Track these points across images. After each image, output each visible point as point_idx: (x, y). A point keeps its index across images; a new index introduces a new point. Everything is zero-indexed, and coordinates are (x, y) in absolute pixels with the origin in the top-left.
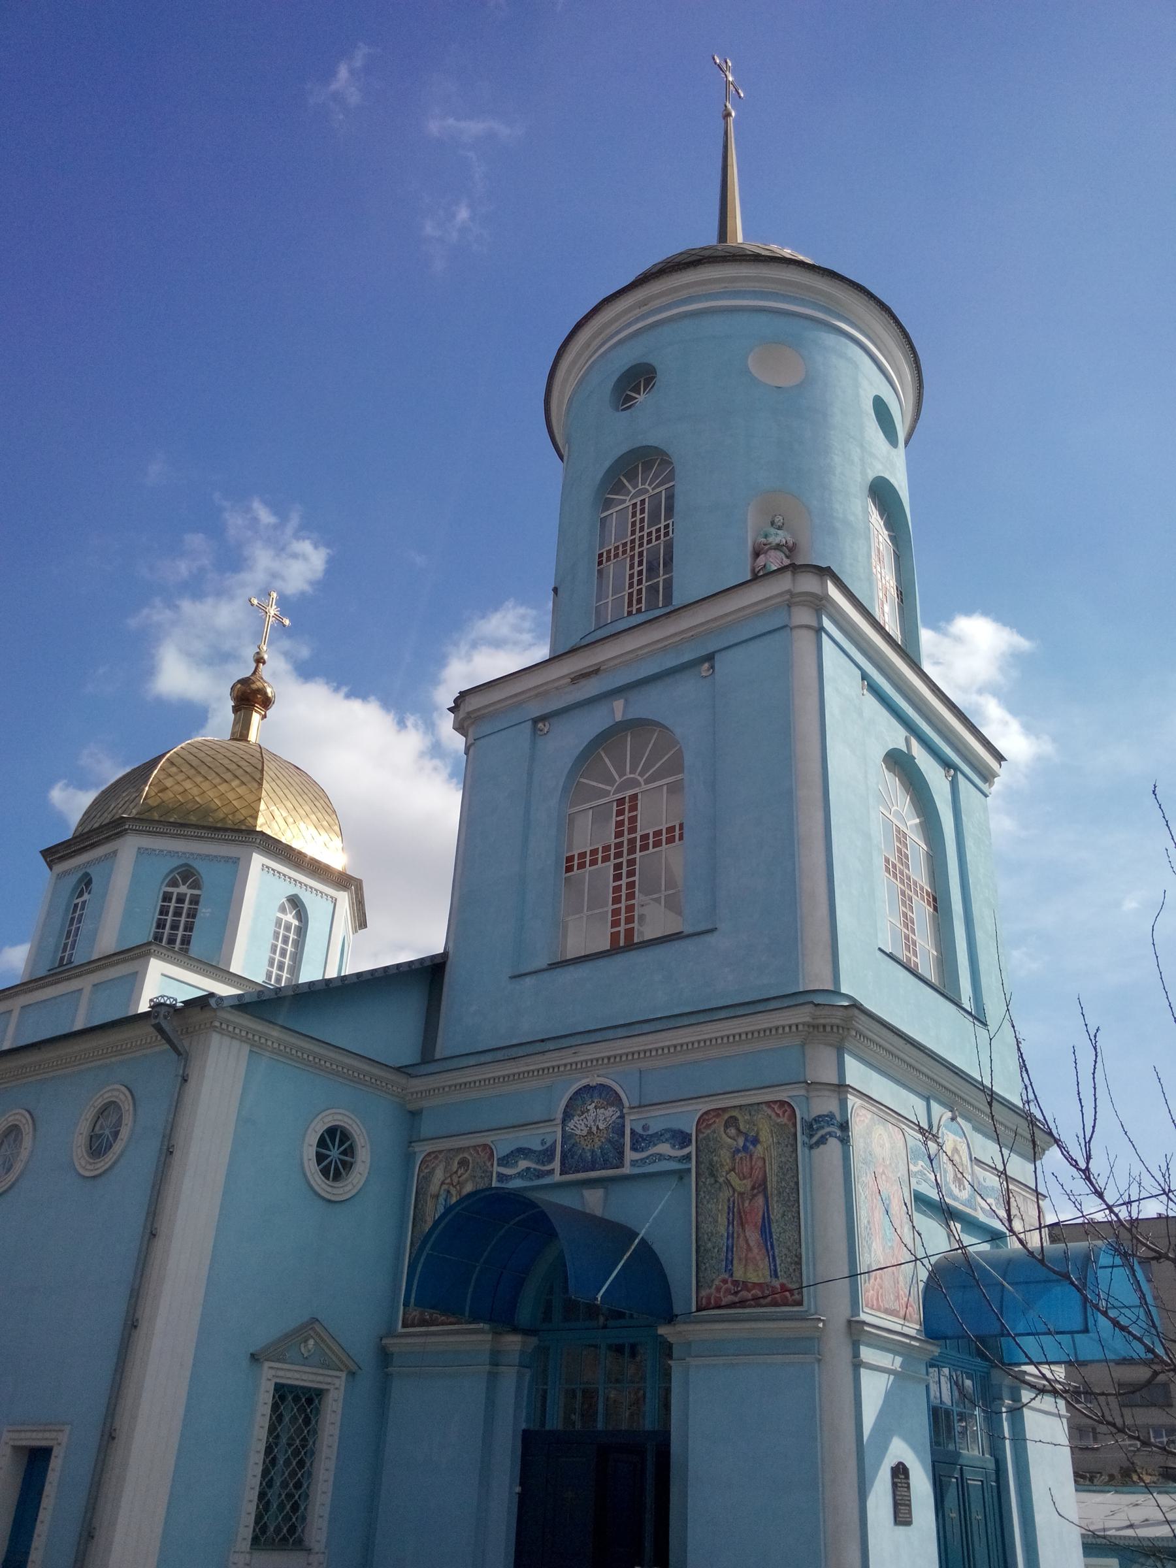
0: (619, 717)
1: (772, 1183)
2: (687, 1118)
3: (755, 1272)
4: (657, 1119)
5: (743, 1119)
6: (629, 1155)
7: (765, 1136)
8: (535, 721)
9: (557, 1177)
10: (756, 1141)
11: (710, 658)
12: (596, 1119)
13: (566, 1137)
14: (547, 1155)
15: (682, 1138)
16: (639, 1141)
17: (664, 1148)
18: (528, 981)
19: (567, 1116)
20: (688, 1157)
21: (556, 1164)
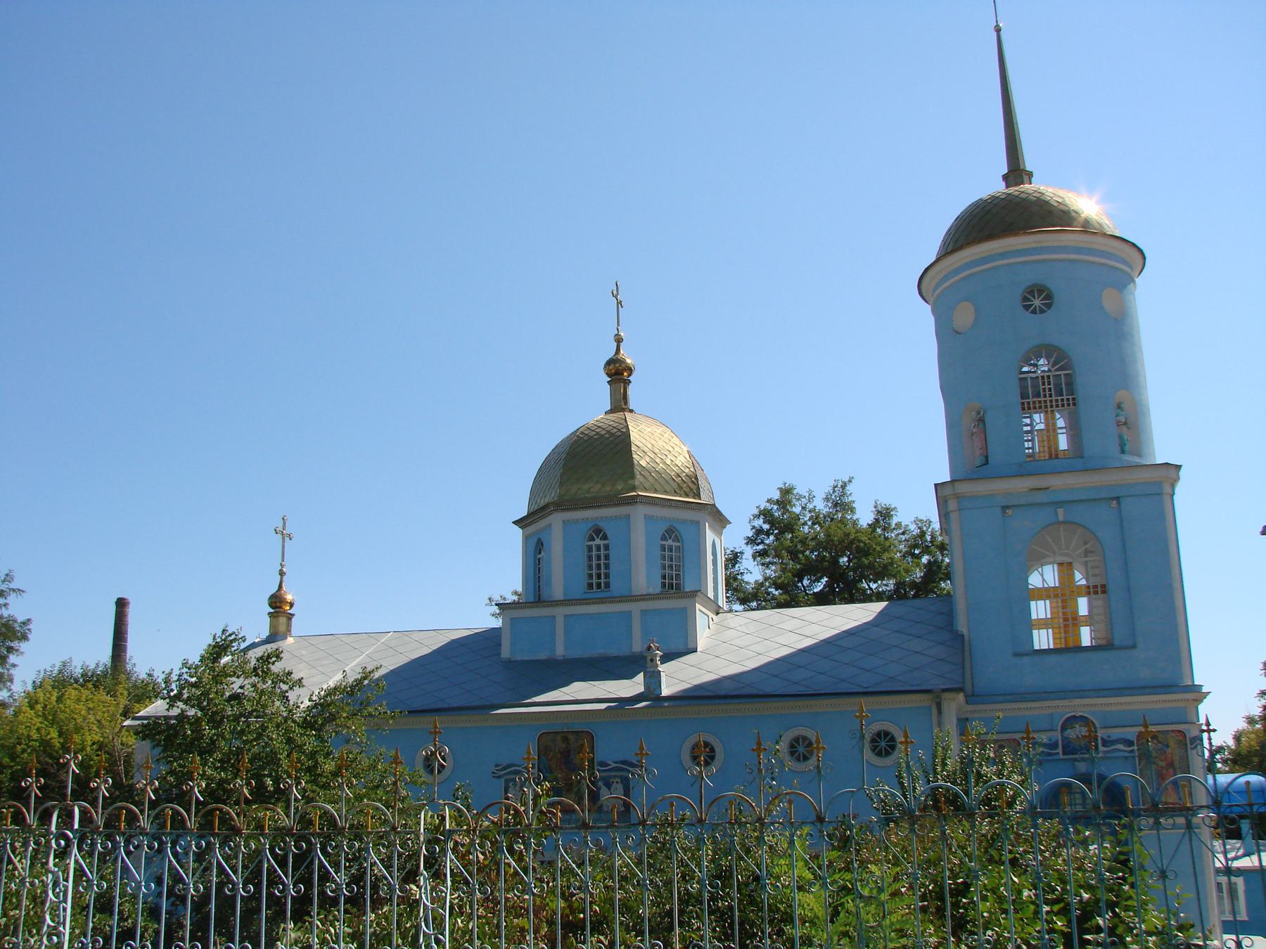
0: (1061, 518)
1: (1177, 764)
2: (1131, 733)
3: (1172, 799)
4: (1116, 733)
5: (1161, 737)
6: (1101, 748)
7: (1172, 744)
8: (1005, 508)
9: (1061, 756)
10: (1167, 746)
11: (1118, 499)
12: (1078, 731)
13: (1064, 739)
14: (1055, 745)
15: (1130, 743)
16: (1105, 743)
17: (1121, 747)
18: (1026, 659)
19: (1063, 728)
20: (1132, 751)
21: (1060, 750)
